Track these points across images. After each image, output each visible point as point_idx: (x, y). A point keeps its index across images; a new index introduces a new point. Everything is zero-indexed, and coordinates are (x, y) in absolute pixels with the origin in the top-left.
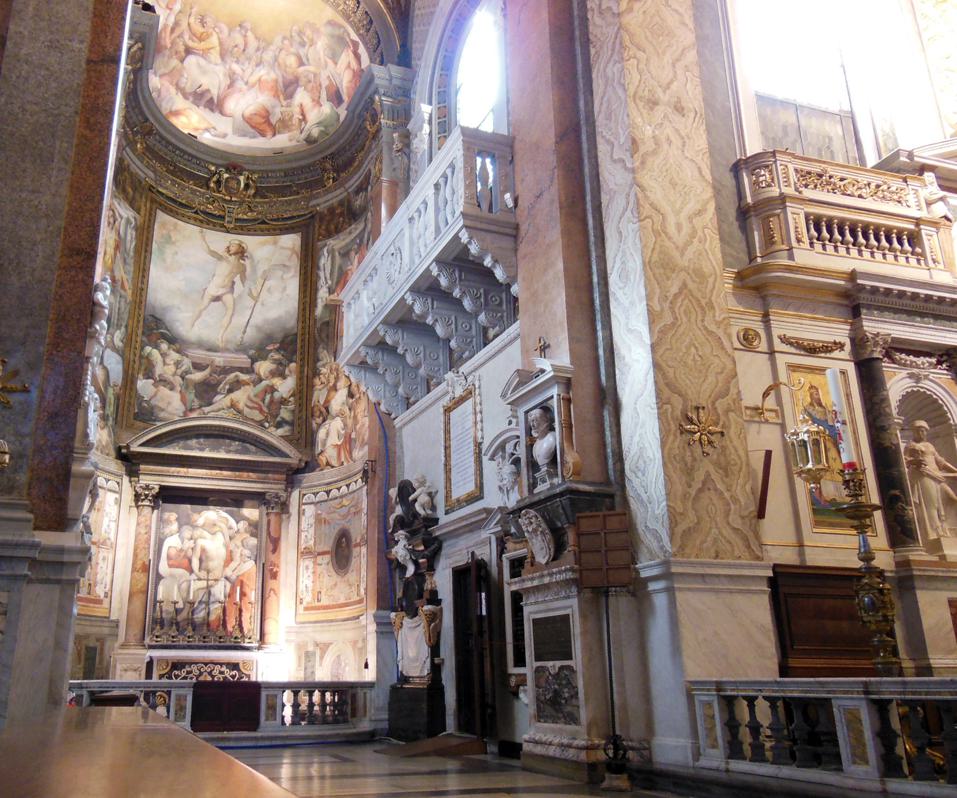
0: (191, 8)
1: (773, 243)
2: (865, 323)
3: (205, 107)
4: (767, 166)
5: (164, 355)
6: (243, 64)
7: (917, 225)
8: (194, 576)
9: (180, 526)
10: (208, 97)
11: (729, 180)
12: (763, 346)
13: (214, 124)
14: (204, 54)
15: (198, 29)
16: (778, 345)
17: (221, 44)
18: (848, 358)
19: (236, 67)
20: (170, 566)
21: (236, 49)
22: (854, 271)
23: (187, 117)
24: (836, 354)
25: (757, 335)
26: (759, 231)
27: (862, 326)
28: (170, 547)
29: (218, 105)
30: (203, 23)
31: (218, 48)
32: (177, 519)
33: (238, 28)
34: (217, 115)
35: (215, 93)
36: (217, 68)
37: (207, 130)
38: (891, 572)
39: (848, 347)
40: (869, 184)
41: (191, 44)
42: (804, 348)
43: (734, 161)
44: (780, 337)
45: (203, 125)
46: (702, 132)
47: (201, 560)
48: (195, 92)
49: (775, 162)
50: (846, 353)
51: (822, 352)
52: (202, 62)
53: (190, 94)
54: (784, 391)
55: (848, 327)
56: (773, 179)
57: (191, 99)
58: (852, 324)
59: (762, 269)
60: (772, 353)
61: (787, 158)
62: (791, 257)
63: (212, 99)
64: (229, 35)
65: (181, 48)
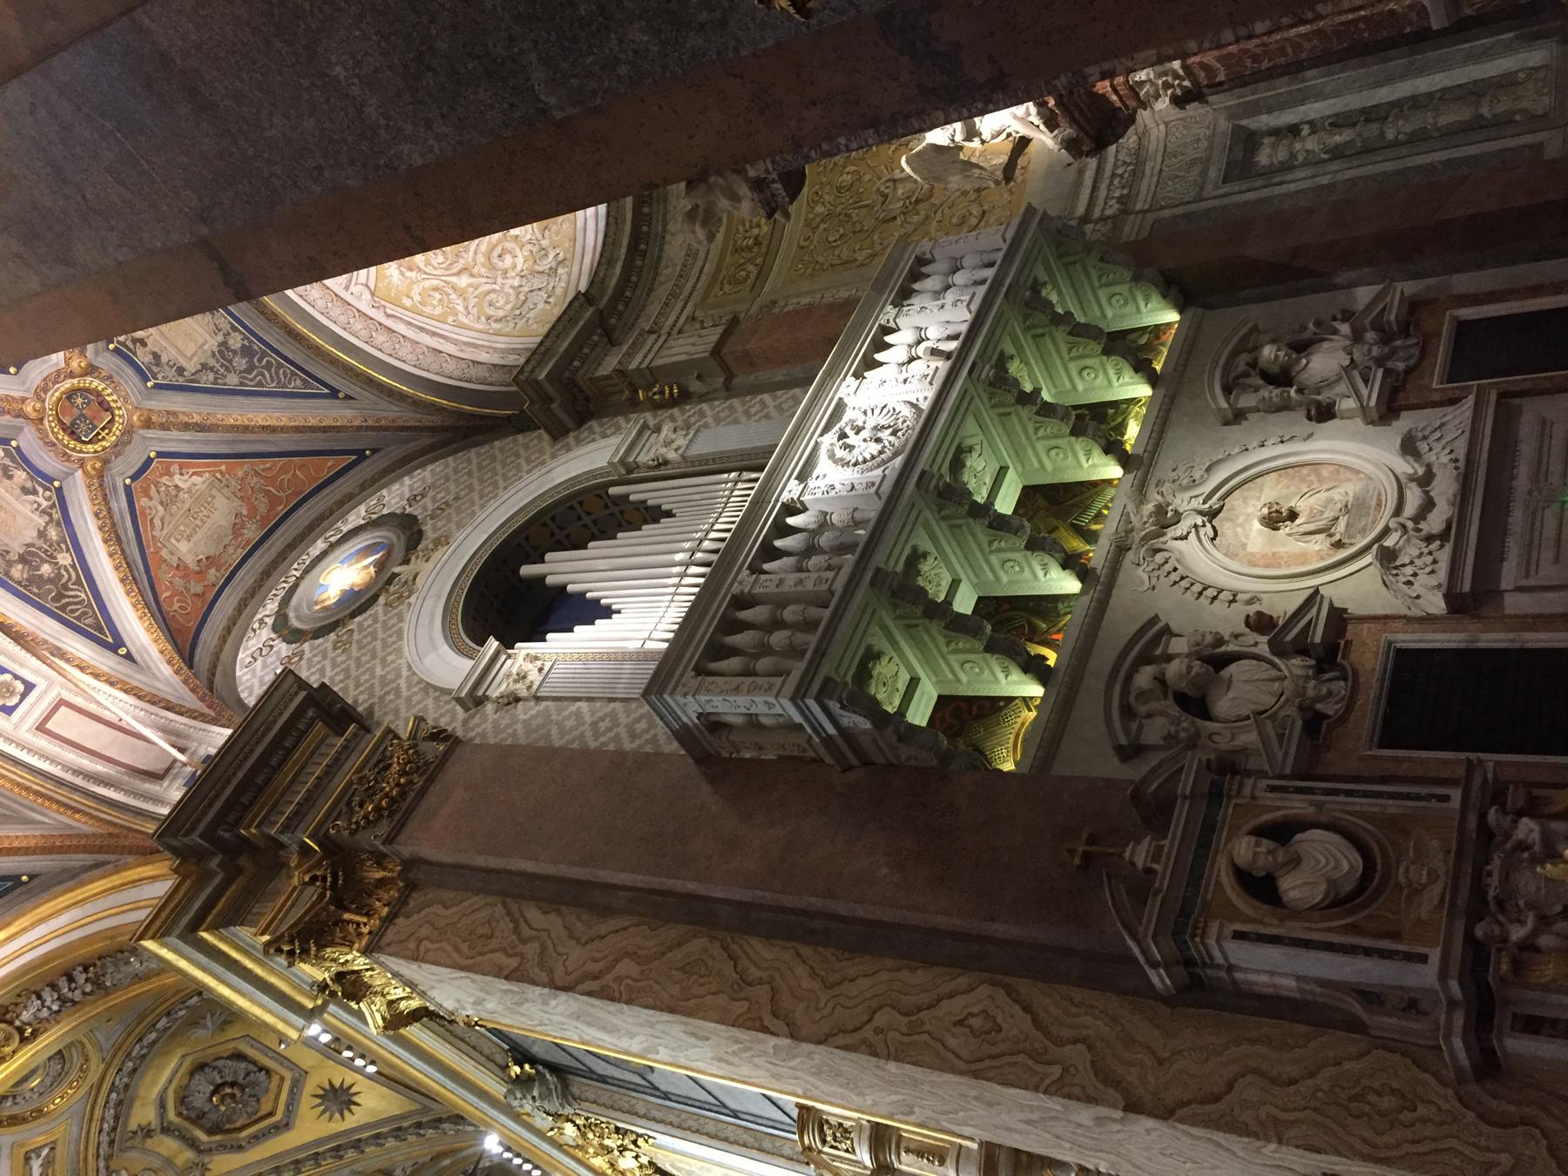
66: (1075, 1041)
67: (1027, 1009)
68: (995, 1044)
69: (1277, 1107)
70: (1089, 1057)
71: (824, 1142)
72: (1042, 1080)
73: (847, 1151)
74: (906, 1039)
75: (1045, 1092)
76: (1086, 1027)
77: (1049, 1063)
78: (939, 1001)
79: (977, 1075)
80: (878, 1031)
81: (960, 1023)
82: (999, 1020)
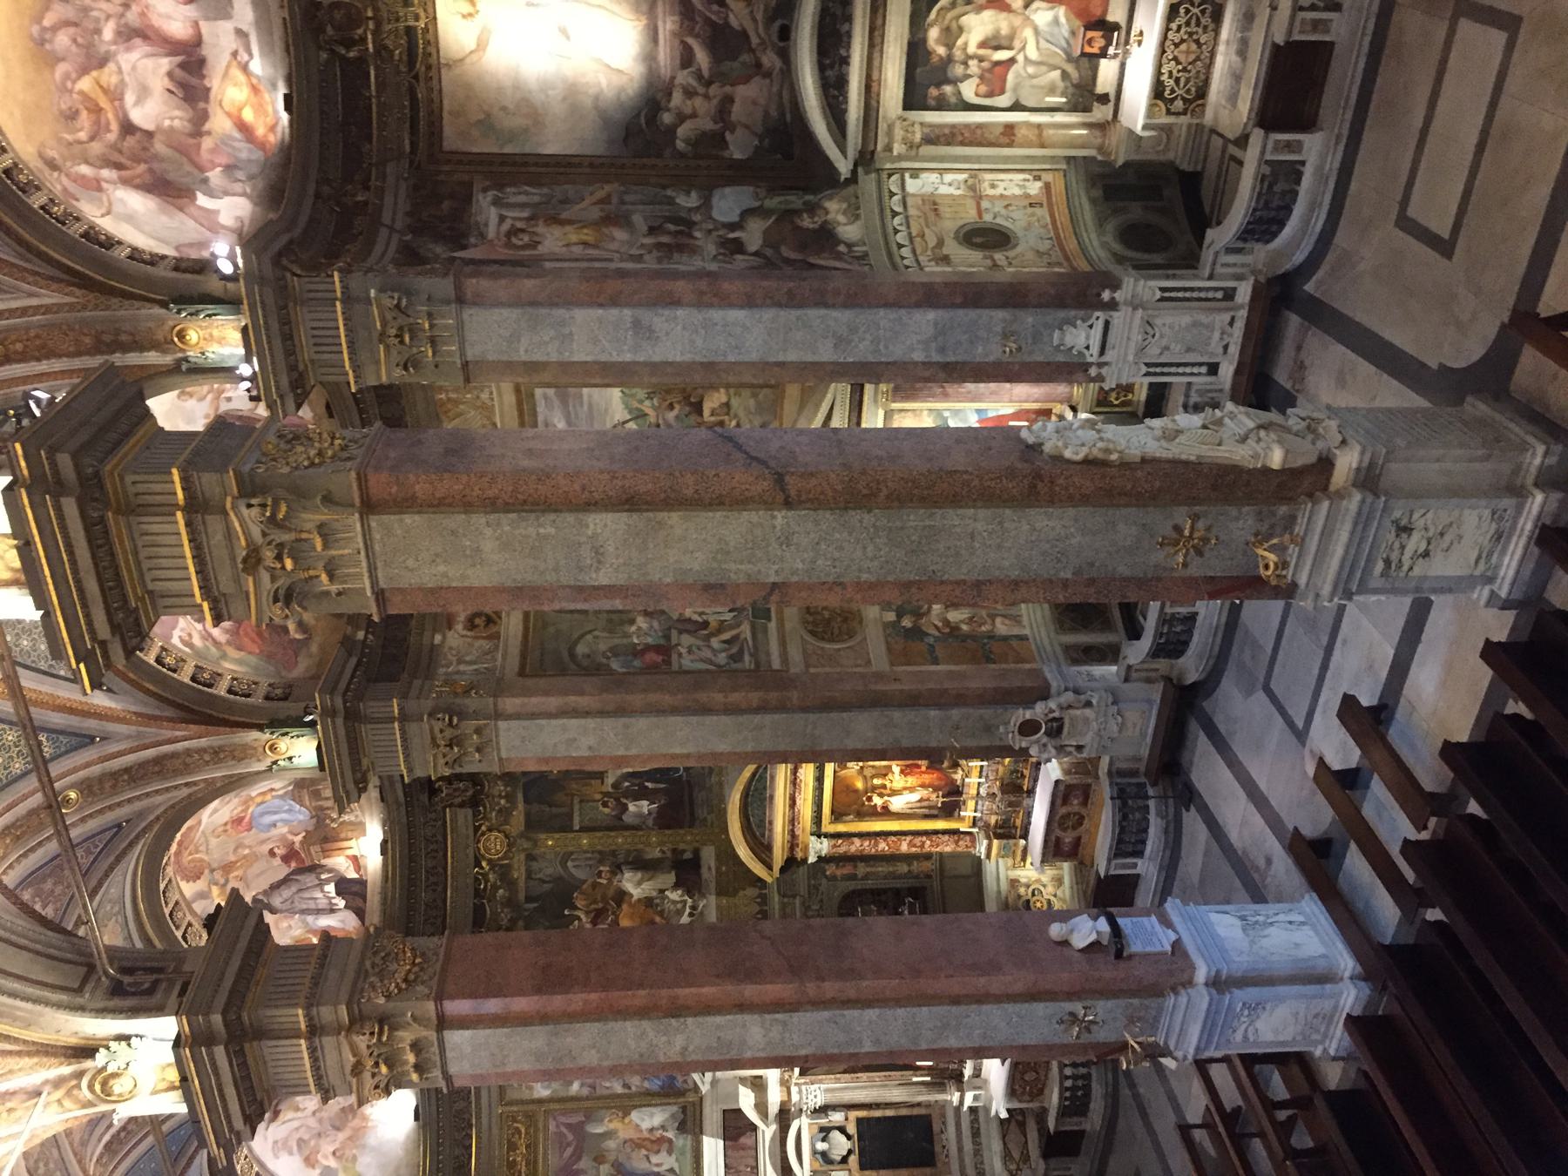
0: (70, 144)
3: (203, 77)
5: (682, 118)
6: (97, 20)
8: (1020, 58)
9: (948, 81)
10: (179, 73)
13: (227, 57)
14: (116, 96)
15: (85, 118)
17: (84, 71)
19: (108, 33)
20: (1002, 92)
21: (80, 40)
23: (240, 110)
28: (977, 95)
29: (189, 54)
30: (72, 116)
31: (95, 73)
32: (938, 85)
33: (48, 46)
34: (206, 51)
35: (165, 63)
36: (126, 67)
37: (245, 68)
41: (114, 126)
45: (241, 77)
47: (998, 48)
48: (185, 99)
52: (130, 98)
53: (194, 108)
57: (202, 105)
63: (182, 66)
64: (63, 59)
65: (130, 141)
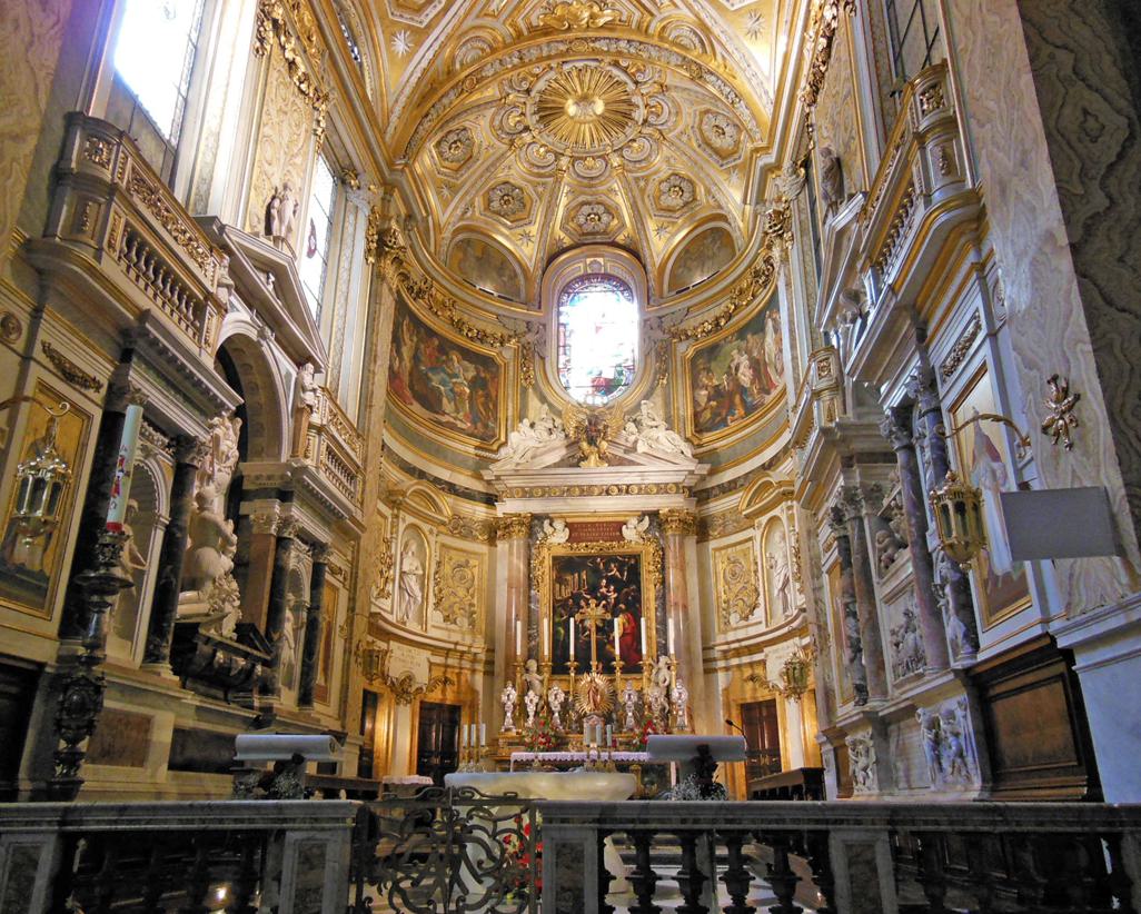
1: (84, 232)
2: (131, 373)
4: (109, 143)
7: (206, 299)
11: (58, 124)
12: (20, 345)
16: (38, 353)
18: (100, 403)
22: (148, 311)
24: (91, 393)
25: (19, 329)
26: (70, 206)
27: (128, 375)
38: (52, 666)
39: (103, 391)
40: (184, 232)
42: (64, 373)
43: (71, 110)
44: (43, 343)
46: (56, 48)
49: (119, 144)
50: (99, 397)
51: (78, 383)
54: (25, 406)
55: (112, 369)
56: (109, 160)
58: (116, 368)
59: (59, 252)
60: (26, 358)
61: (130, 149)
62: (98, 258)
66: (1109, 197)
67: (1120, 156)
68: (1080, 140)
69: (1122, 343)
70: (1101, 210)
71: (923, 94)
72: (1067, 182)
73: (923, 111)
74: (1054, 78)
75: (1058, 188)
76: (1125, 200)
77: (1083, 183)
78: (1097, 91)
79: (1049, 136)
80: (1052, 56)
81: (1086, 112)
82: (1100, 140)
